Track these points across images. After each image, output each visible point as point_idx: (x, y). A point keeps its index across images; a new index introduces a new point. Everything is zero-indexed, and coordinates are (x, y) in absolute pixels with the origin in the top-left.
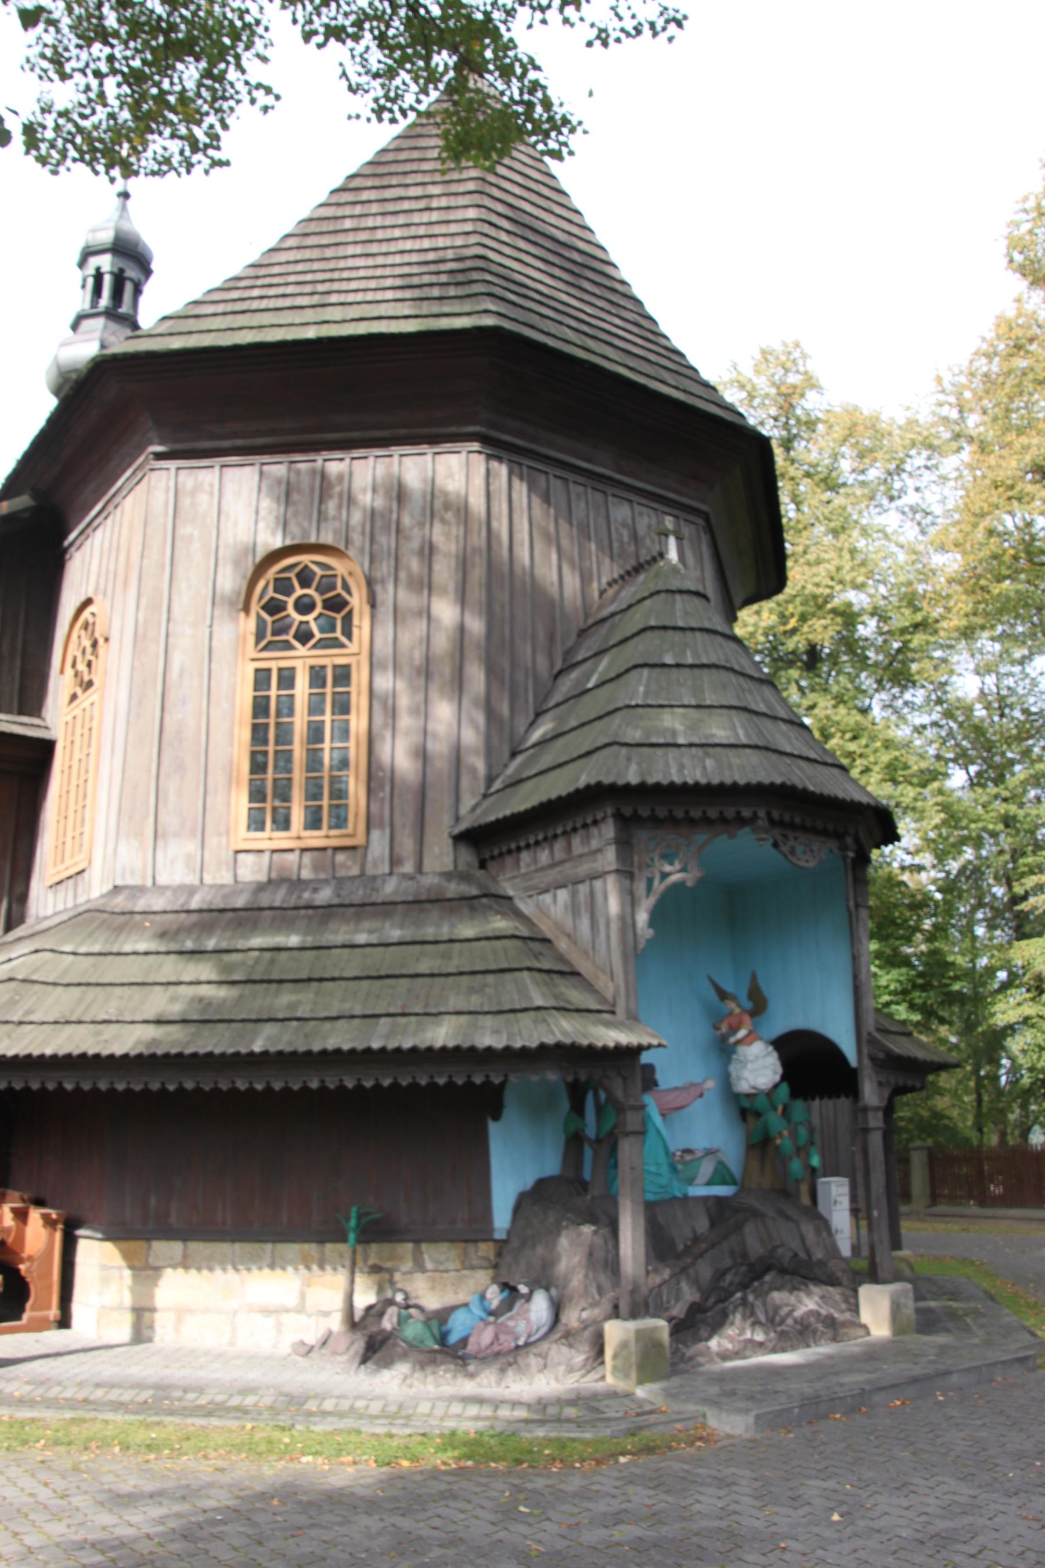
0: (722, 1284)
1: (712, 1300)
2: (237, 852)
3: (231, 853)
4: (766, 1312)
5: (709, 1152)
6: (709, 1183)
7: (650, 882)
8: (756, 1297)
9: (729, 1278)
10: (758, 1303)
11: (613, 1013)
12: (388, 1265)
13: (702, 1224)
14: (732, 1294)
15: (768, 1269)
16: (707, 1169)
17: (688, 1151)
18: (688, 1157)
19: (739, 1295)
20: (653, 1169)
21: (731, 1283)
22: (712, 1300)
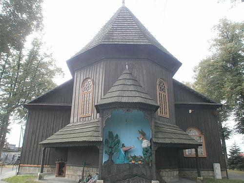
15: (136, 176)
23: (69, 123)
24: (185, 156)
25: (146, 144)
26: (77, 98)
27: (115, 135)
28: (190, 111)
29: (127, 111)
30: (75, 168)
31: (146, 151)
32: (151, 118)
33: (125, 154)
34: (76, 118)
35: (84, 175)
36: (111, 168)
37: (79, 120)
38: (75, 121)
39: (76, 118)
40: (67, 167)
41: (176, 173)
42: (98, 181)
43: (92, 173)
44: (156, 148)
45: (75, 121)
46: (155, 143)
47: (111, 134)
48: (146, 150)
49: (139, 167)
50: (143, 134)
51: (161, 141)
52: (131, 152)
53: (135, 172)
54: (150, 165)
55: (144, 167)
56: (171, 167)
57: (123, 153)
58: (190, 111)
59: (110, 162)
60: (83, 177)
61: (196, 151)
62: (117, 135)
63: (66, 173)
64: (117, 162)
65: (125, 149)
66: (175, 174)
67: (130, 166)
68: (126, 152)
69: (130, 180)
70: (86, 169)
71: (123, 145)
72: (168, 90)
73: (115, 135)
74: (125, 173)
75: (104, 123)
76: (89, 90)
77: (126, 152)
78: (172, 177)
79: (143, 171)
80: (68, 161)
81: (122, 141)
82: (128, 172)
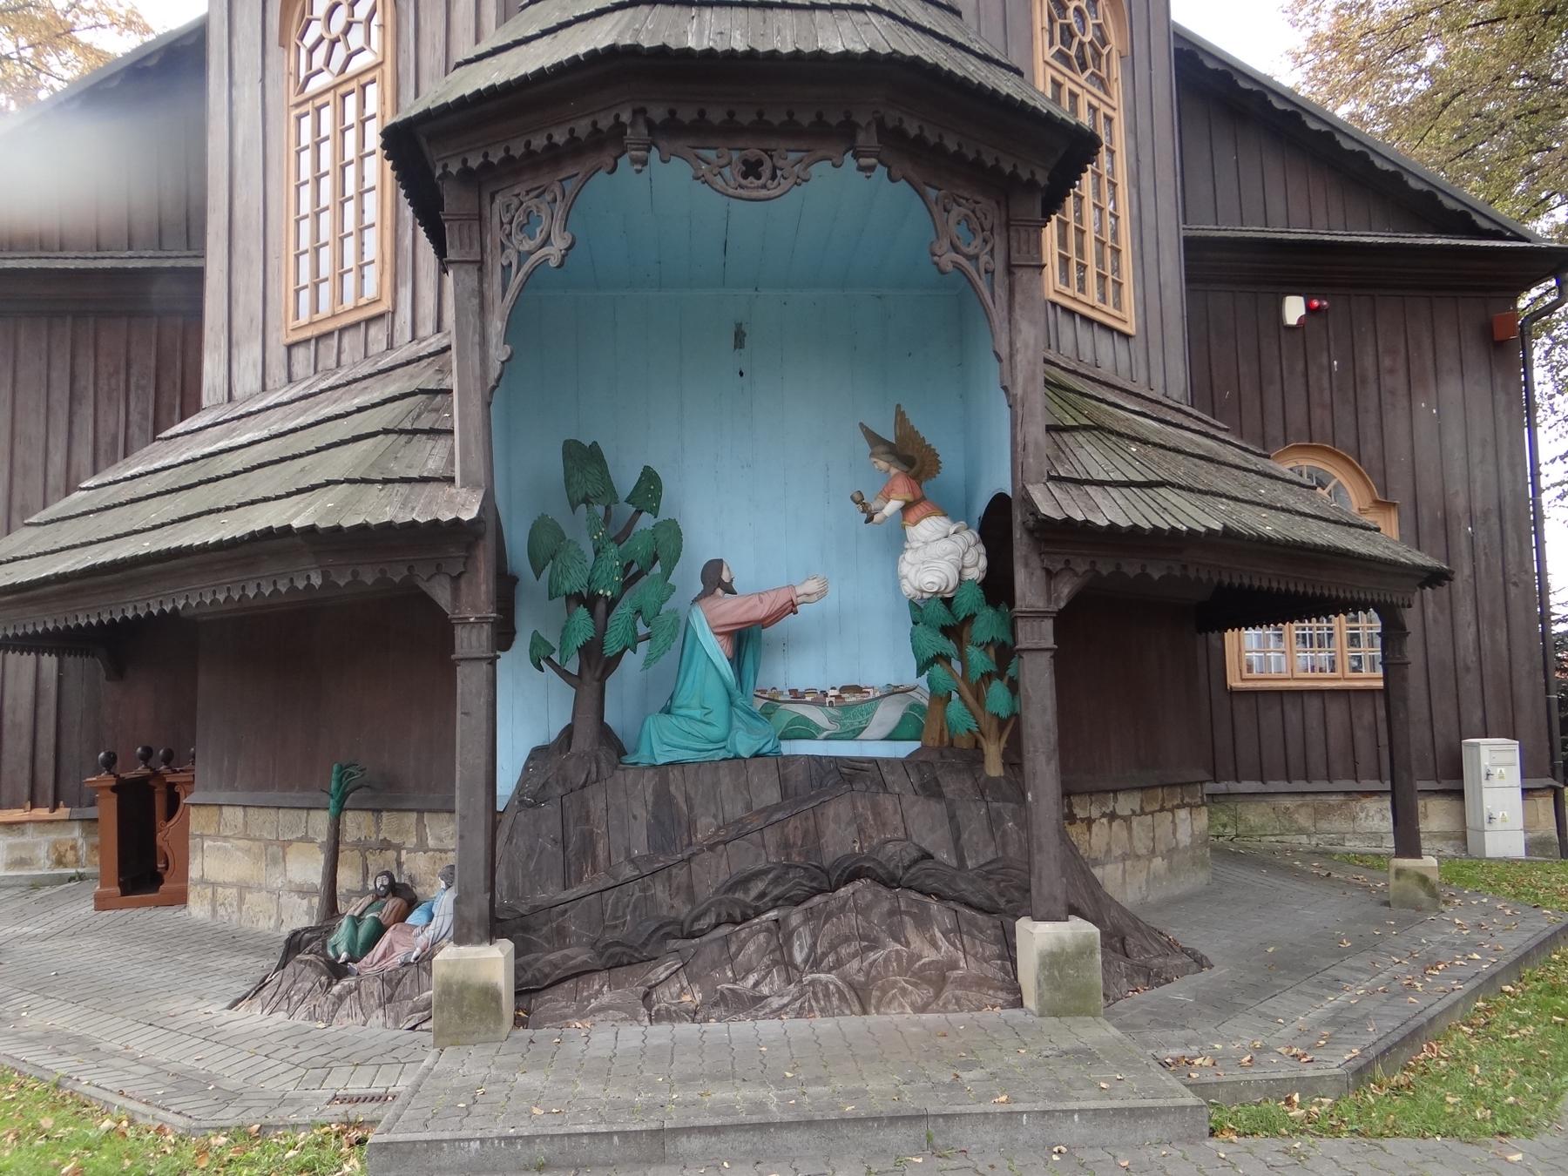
0: (739, 895)
1: (703, 924)
2: (290, 347)
3: (283, 350)
4: (813, 946)
5: (893, 691)
6: (890, 737)
7: (506, 269)
8: (806, 921)
9: (758, 887)
10: (805, 932)
11: (451, 480)
12: (396, 840)
13: (771, 795)
14: (758, 913)
16: (888, 715)
17: (857, 689)
18: (850, 698)
19: (772, 914)
20: (697, 713)
21: (762, 895)
22: (711, 919)
23: (190, 403)
24: (1234, 682)
25: (939, 556)
26: (249, 161)
27: (626, 479)
28: (1294, 309)
29: (751, 169)
30: (266, 822)
31: (947, 631)
32: (1010, 269)
33: (737, 660)
34: (249, 355)
35: (347, 878)
36: (597, 805)
37: (277, 372)
38: (247, 380)
39: (249, 355)
40: (197, 820)
41: (1188, 825)
42: (449, 953)
43: (417, 865)
44: (1065, 590)
45: (247, 380)
46: (1063, 537)
47: (584, 460)
48: (942, 622)
49: (884, 786)
50: (912, 459)
51: (1109, 510)
52: (785, 644)
53: (839, 835)
54: (994, 767)
55: (931, 790)
56: (1161, 780)
57: (716, 649)
58: (1294, 309)
59: (587, 753)
60: (331, 909)
61: (1393, 634)
62: (650, 484)
63: (194, 872)
64: (663, 743)
65: (731, 609)
66: (1184, 838)
67: (784, 784)
68: (744, 641)
69: (795, 919)
70: (356, 825)
71: (714, 579)
72: (1129, 60)
73: (626, 479)
74: (745, 858)
75: (497, 326)
76: (357, 64)
77: (744, 641)
78: (1158, 863)
79: (924, 826)
80: (203, 770)
81: (701, 544)
82: (771, 837)
